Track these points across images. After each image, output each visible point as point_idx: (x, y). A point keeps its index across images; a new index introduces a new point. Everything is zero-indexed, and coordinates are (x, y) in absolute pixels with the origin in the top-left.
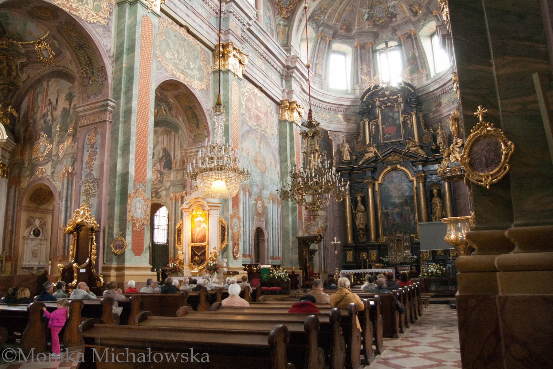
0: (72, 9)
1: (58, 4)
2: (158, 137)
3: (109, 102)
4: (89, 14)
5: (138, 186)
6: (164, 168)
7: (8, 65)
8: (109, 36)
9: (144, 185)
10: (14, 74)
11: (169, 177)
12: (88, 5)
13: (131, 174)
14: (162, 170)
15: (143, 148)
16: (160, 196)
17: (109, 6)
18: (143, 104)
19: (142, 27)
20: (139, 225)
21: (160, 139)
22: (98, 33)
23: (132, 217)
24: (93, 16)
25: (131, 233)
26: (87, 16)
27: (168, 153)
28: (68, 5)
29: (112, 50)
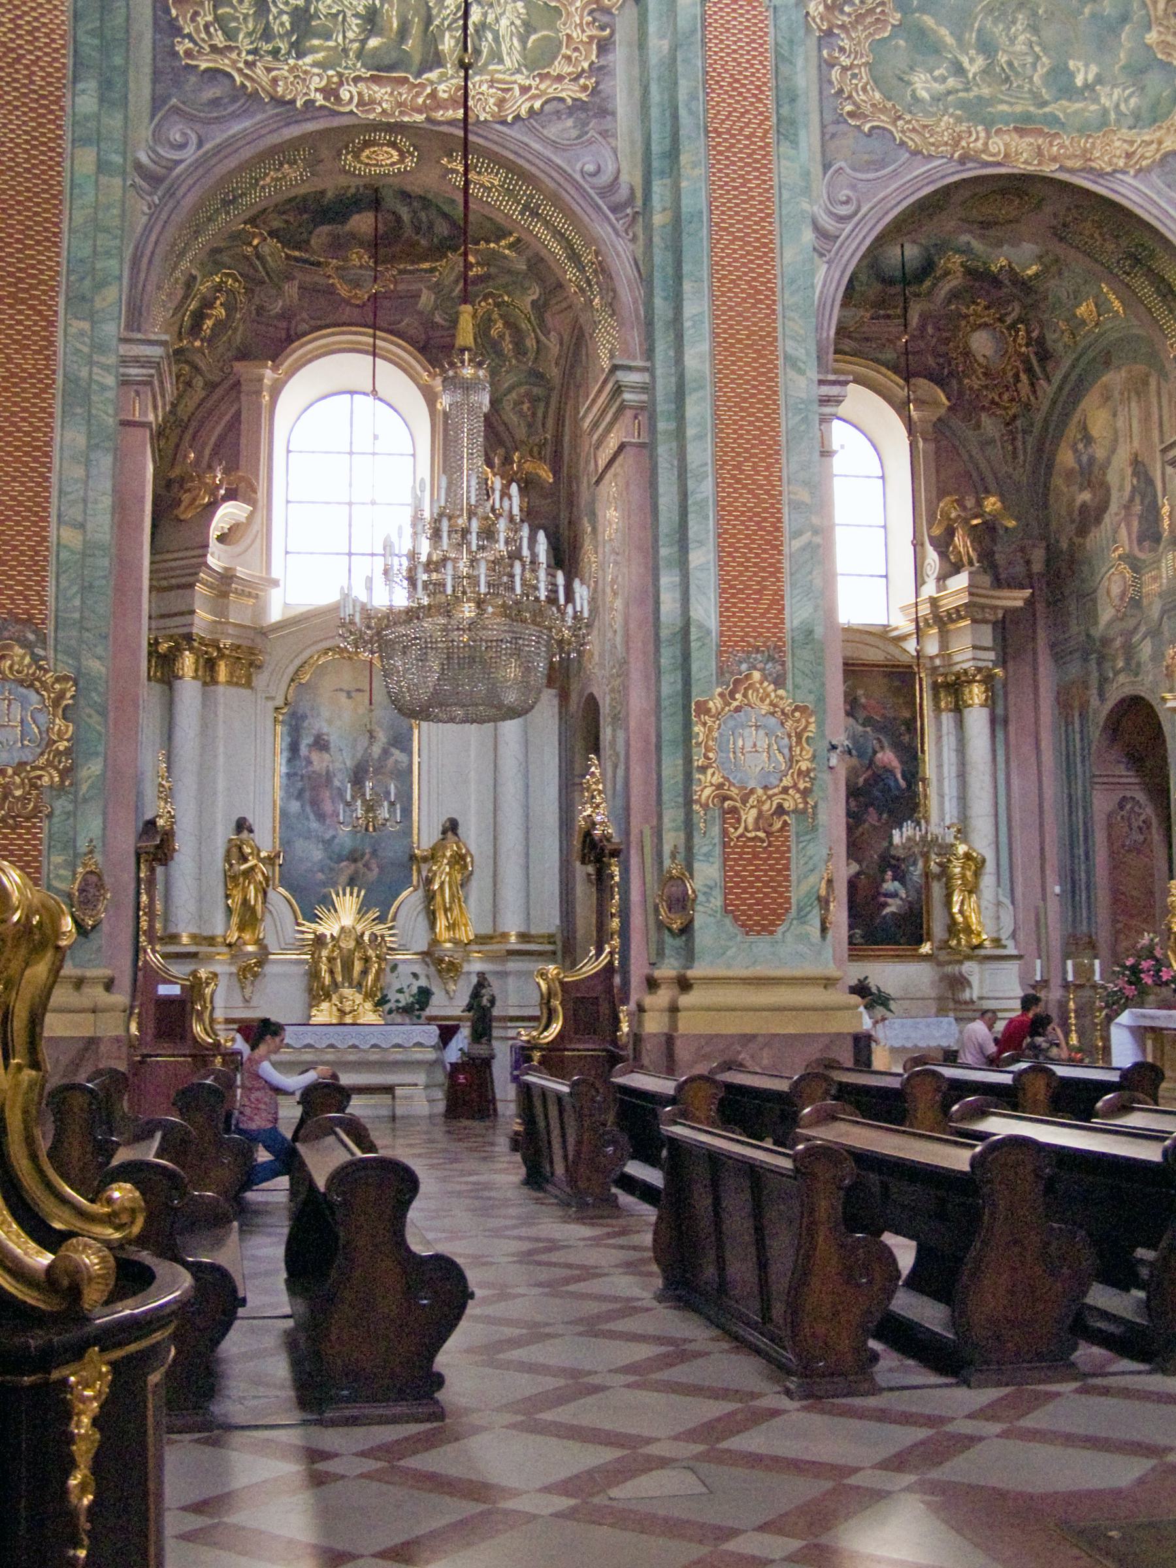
0: (439, 105)
1: (384, 111)
2: (1115, 415)
3: (621, 375)
4: (508, 90)
5: (744, 667)
6: (1140, 542)
7: (507, 324)
8: (604, 134)
9: (771, 659)
10: (530, 343)
11: (1155, 579)
12: (501, 61)
13: (701, 626)
14: (1137, 552)
15: (757, 514)
16: (1139, 665)
17: (595, 20)
18: (740, 341)
19: (704, 44)
20: (760, 814)
21: (1120, 423)
22: (554, 145)
23: (720, 786)
24: (525, 89)
25: (718, 850)
26: (501, 103)
27: (1146, 474)
28: (420, 101)
29: (624, 178)
